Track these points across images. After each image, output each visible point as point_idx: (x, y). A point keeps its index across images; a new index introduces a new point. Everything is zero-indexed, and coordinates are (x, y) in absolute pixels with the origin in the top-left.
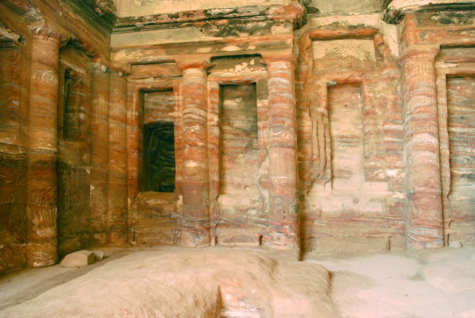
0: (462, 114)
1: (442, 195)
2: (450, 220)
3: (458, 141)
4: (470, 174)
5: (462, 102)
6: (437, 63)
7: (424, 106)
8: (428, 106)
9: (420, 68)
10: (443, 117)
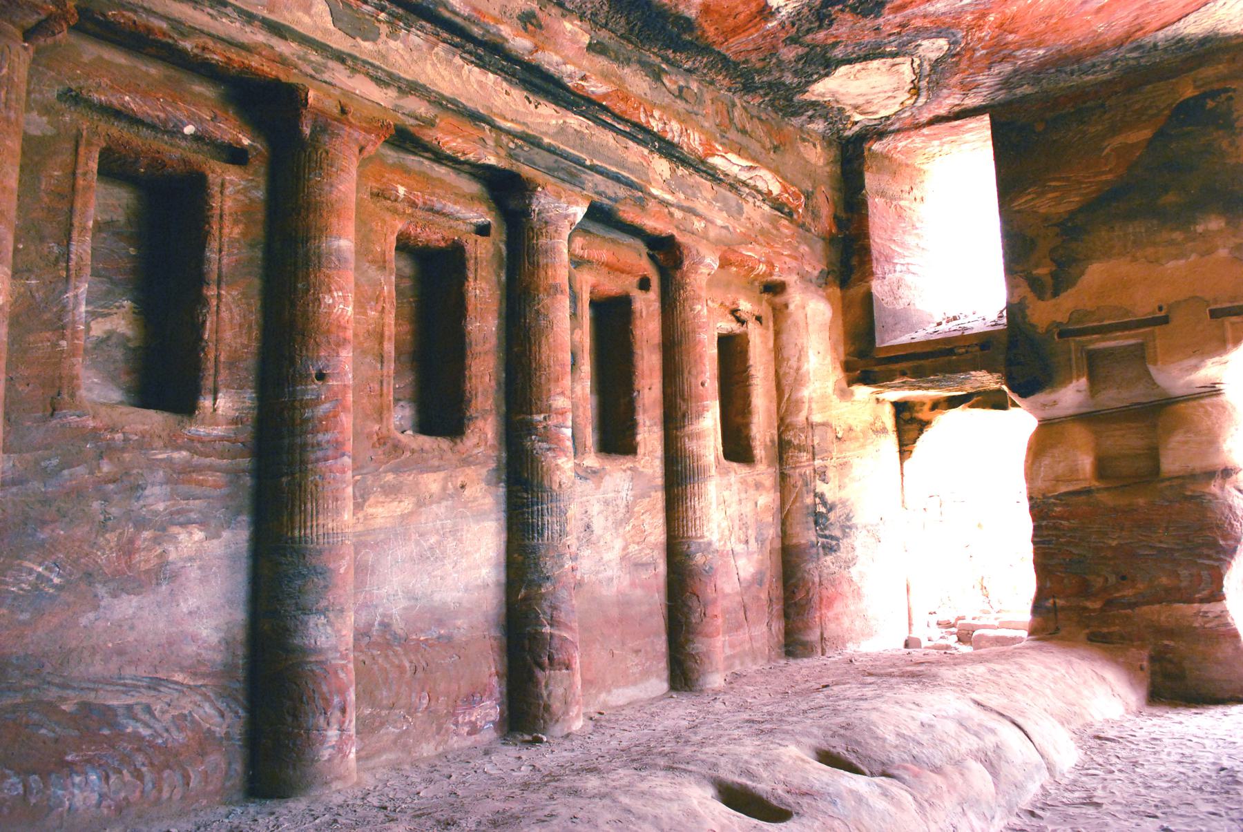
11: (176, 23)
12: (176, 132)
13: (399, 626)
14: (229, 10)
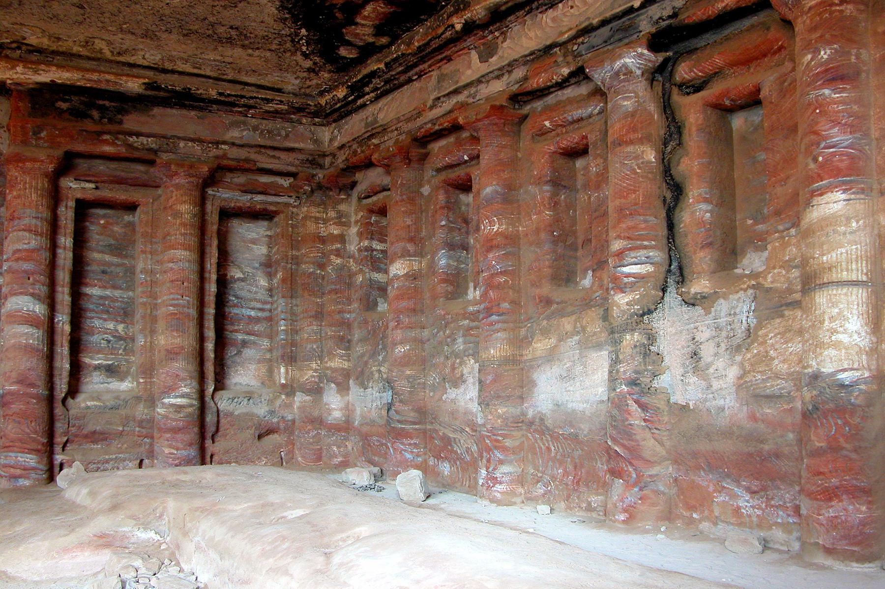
0: (103, 265)
1: (50, 399)
2: (65, 439)
3: (93, 310)
4: (109, 366)
5: (105, 246)
6: (62, 179)
7: (26, 250)
8: (33, 251)
9: (27, 186)
10: (64, 269)
11: (433, 122)
12: (466, 162)
13: (549, 423)
14: (442, 99)
